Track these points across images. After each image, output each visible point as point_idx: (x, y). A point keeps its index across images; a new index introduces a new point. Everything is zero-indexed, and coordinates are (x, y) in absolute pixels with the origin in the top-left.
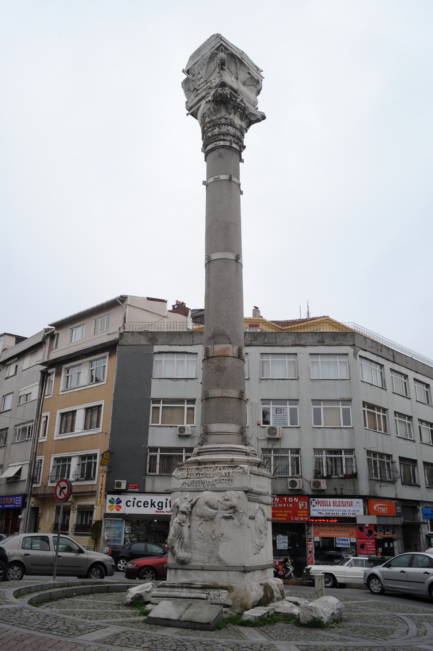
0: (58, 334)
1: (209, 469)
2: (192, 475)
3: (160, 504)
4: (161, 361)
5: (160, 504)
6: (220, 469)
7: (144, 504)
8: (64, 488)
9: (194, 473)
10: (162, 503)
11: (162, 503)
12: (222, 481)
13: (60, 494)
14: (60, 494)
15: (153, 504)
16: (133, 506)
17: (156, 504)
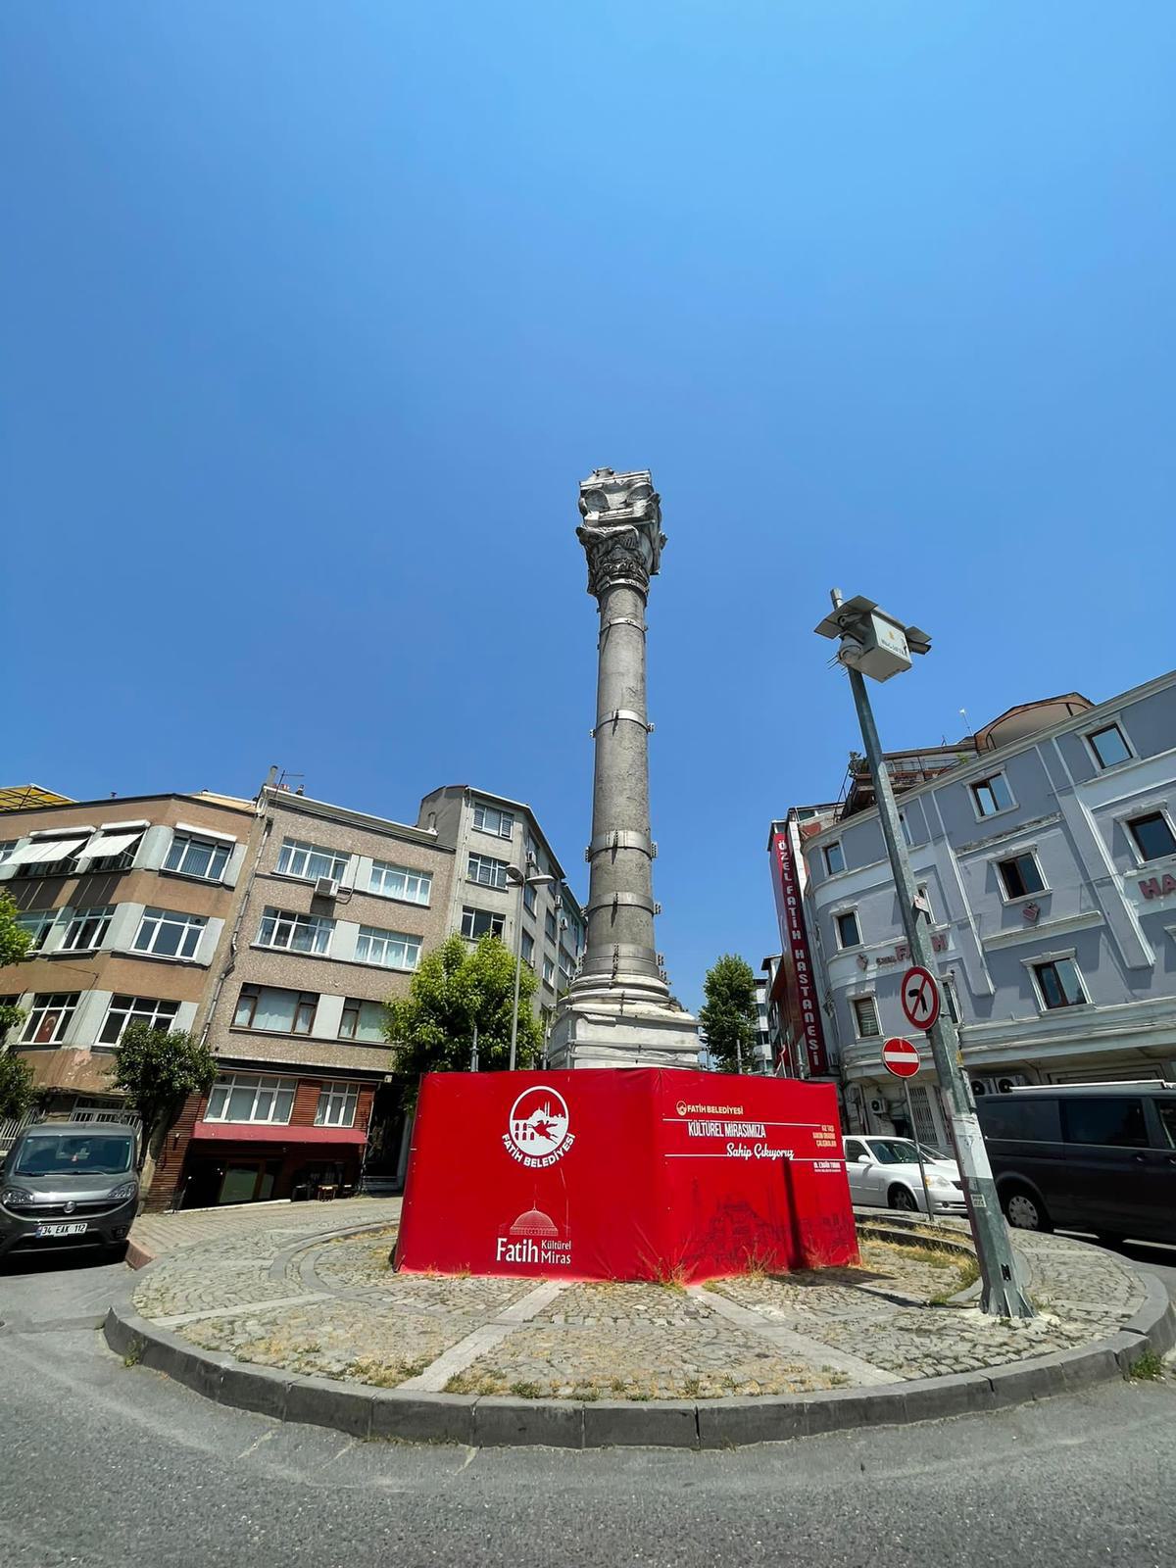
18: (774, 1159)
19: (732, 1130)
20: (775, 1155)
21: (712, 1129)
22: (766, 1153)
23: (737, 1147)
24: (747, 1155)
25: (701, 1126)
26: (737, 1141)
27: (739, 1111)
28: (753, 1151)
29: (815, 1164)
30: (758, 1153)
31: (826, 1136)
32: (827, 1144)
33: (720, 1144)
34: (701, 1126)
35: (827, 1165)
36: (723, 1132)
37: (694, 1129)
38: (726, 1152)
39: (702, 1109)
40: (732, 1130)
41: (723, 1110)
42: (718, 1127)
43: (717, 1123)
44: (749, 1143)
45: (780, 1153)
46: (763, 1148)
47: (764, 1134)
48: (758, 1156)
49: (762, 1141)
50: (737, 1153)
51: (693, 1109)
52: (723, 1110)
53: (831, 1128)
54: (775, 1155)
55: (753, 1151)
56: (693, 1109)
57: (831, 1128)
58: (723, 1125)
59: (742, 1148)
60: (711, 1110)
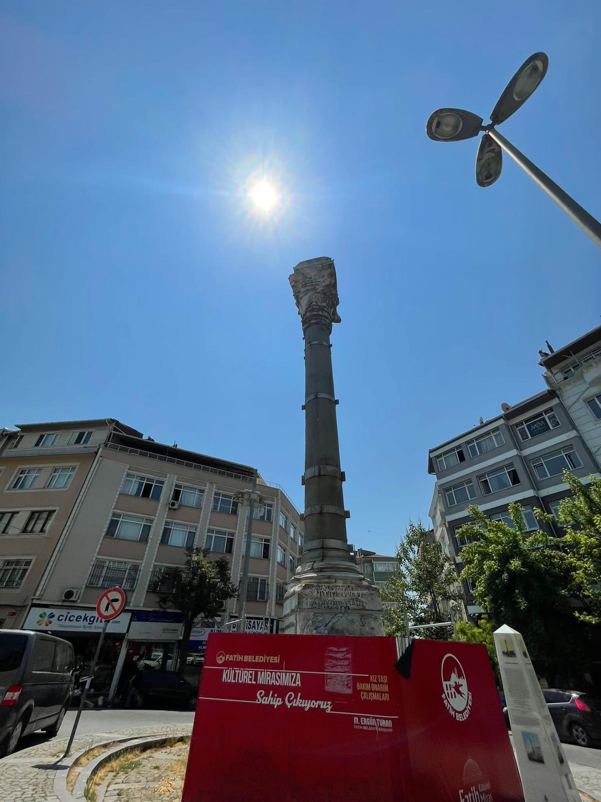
0: (22, 437)
1: (341, 587)
2: (322, 593)
3: (92, 619)
4: (132, 481)
5: (92, 619)
6: (352, 589)
7: (77, 618)
8: (117, 600)
9: (324, 591)
10: (94, 617)
11: (94, 617)
12: (356, 603)
13: (107, 609)
14: (107, 609)
15: (85, 619)
16: (65, 620)
17: (88, 619)
18: (306, 709)
19: (265, 677)
20: (308, 705)
21: (245, 677)
22: (298, 703)
23: (267, 695)
24: (277, 702)
25: (235, 674)
26: (268, 689)
27: (276, 660)
28: (283, 700)
29: (356, 719)
30: (290, 701)
31: (375, 687)
32: (375, 697)
33: (250, 690)
34: (235, 674)
35: (384, 723)
36: (256, 679)
37: (228, 676)
38: (255, 698)
39: (239, 658)
40: (265, 677)
41: (259, 659)
42: (251, 675)
43: (252, 671)
44: (281, 691)
45: (314, 704)
46: (296, 697)
47: (299, 683)
48: (289, 705)
49: (296, 690)
50: (266, 701)
51: (230, 658)
52: (259, 659)
53: (384, 679)
54: (308, 705)
55: (283, 700)
56: (230, 658)
57: (384, 679)
58: (256, 673)
59: (273, 696)
60: (248, 658)
